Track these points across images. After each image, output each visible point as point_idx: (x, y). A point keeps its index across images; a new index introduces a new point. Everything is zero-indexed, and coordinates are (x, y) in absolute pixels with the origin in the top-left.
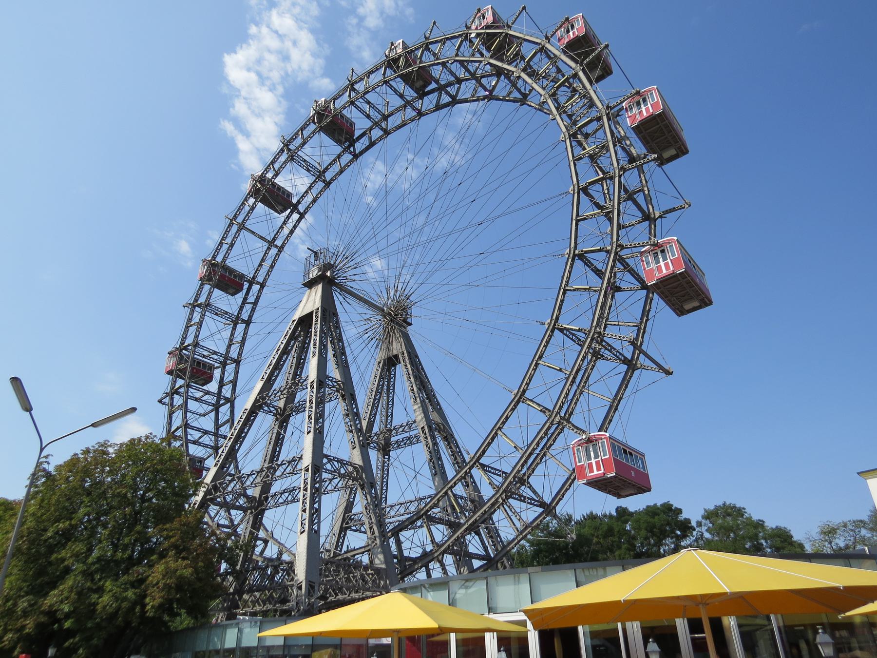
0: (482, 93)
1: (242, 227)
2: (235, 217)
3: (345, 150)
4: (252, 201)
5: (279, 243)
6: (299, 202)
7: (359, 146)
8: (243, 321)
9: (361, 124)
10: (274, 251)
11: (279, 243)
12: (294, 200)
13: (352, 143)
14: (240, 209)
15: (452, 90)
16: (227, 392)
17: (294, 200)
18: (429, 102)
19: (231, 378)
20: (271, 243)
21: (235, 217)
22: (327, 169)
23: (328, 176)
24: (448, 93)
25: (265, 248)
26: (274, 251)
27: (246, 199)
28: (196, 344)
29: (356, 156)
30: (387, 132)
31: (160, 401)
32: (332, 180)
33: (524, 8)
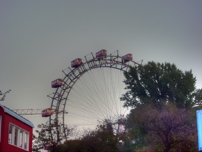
31: (142, 60)
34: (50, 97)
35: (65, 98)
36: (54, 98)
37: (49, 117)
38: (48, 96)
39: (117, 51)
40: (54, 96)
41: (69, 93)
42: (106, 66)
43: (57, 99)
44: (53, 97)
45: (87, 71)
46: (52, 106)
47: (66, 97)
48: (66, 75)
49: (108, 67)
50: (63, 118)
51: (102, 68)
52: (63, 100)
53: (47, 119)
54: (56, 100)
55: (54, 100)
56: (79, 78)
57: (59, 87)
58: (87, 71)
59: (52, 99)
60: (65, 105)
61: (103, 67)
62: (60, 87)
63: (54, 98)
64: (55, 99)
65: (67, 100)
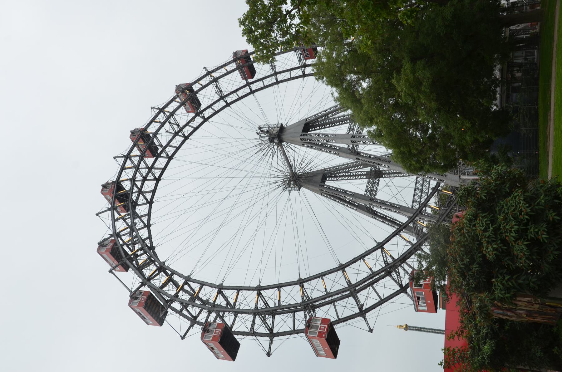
1: (215, 80)
2: (213, 71)
5: (229, 100)
8: (184, 136)
10: (222, 103)
11: (229, 100)
14: (218, 69)
16: (157, 173)
19: (162, 166)
20: (222, 98)
21: (213, 71)
22: (280, 73)
23: (280, 77)
25: (217, 99)
26: (222, 103)
28: (155, 134)
29: (304, 75)
34: (270, 348)
35: (259, 294)
36: (272, 335)
37: (334, 326)
38: (269, 354)
39: (97, 215)
40: (262, 335)
41: (239, 289)
42: (150, 237)
43: (269, 320)
44: (268, 339)
45: (164, 263)
46: (295, 331)
47: (255, 292)
48: (192, 326)
49: (149, 231)
50: (322, 275)
51: (154, 245)
52: (266, 304)
53: (339, 329)
54: (273, 326)
55: (275, 331)
56: (188, 280)
57: (233, 330)
58: (164, 263)
59: (275, 338)
60: (279, 286)
61: (151, 242)
62: (232, 327)
63: (272, 335)
64: (271, 330)
65: (262, 285)
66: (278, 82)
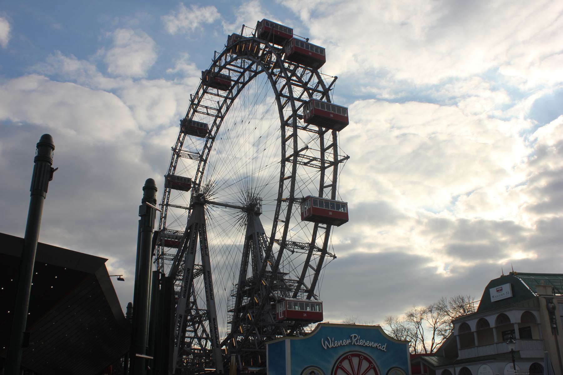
0: (253, 74)
1: (167, 205)
2: (163, 202)
3: (209, 138)
4: (168, 190)
6: (196, 179)
7: (213, 133)
9: (209, 121)
12: (193, 180)
13: (210, 133)
15: (241, 80)
17: (193, 180)
18: (235, 91)
21: (163, 202)
23: (204, 158)
24: (241, 83)
27: (165, 190)
30: (222, 118)
32: (207, 158)
33: (244, 26)
66: (205, 161)
